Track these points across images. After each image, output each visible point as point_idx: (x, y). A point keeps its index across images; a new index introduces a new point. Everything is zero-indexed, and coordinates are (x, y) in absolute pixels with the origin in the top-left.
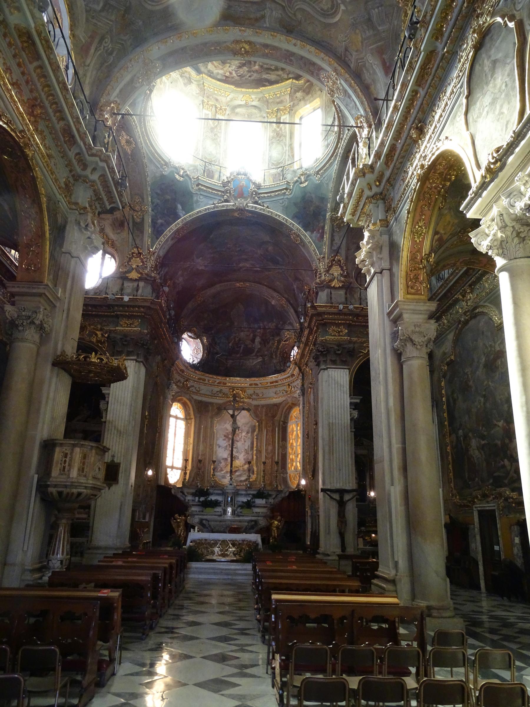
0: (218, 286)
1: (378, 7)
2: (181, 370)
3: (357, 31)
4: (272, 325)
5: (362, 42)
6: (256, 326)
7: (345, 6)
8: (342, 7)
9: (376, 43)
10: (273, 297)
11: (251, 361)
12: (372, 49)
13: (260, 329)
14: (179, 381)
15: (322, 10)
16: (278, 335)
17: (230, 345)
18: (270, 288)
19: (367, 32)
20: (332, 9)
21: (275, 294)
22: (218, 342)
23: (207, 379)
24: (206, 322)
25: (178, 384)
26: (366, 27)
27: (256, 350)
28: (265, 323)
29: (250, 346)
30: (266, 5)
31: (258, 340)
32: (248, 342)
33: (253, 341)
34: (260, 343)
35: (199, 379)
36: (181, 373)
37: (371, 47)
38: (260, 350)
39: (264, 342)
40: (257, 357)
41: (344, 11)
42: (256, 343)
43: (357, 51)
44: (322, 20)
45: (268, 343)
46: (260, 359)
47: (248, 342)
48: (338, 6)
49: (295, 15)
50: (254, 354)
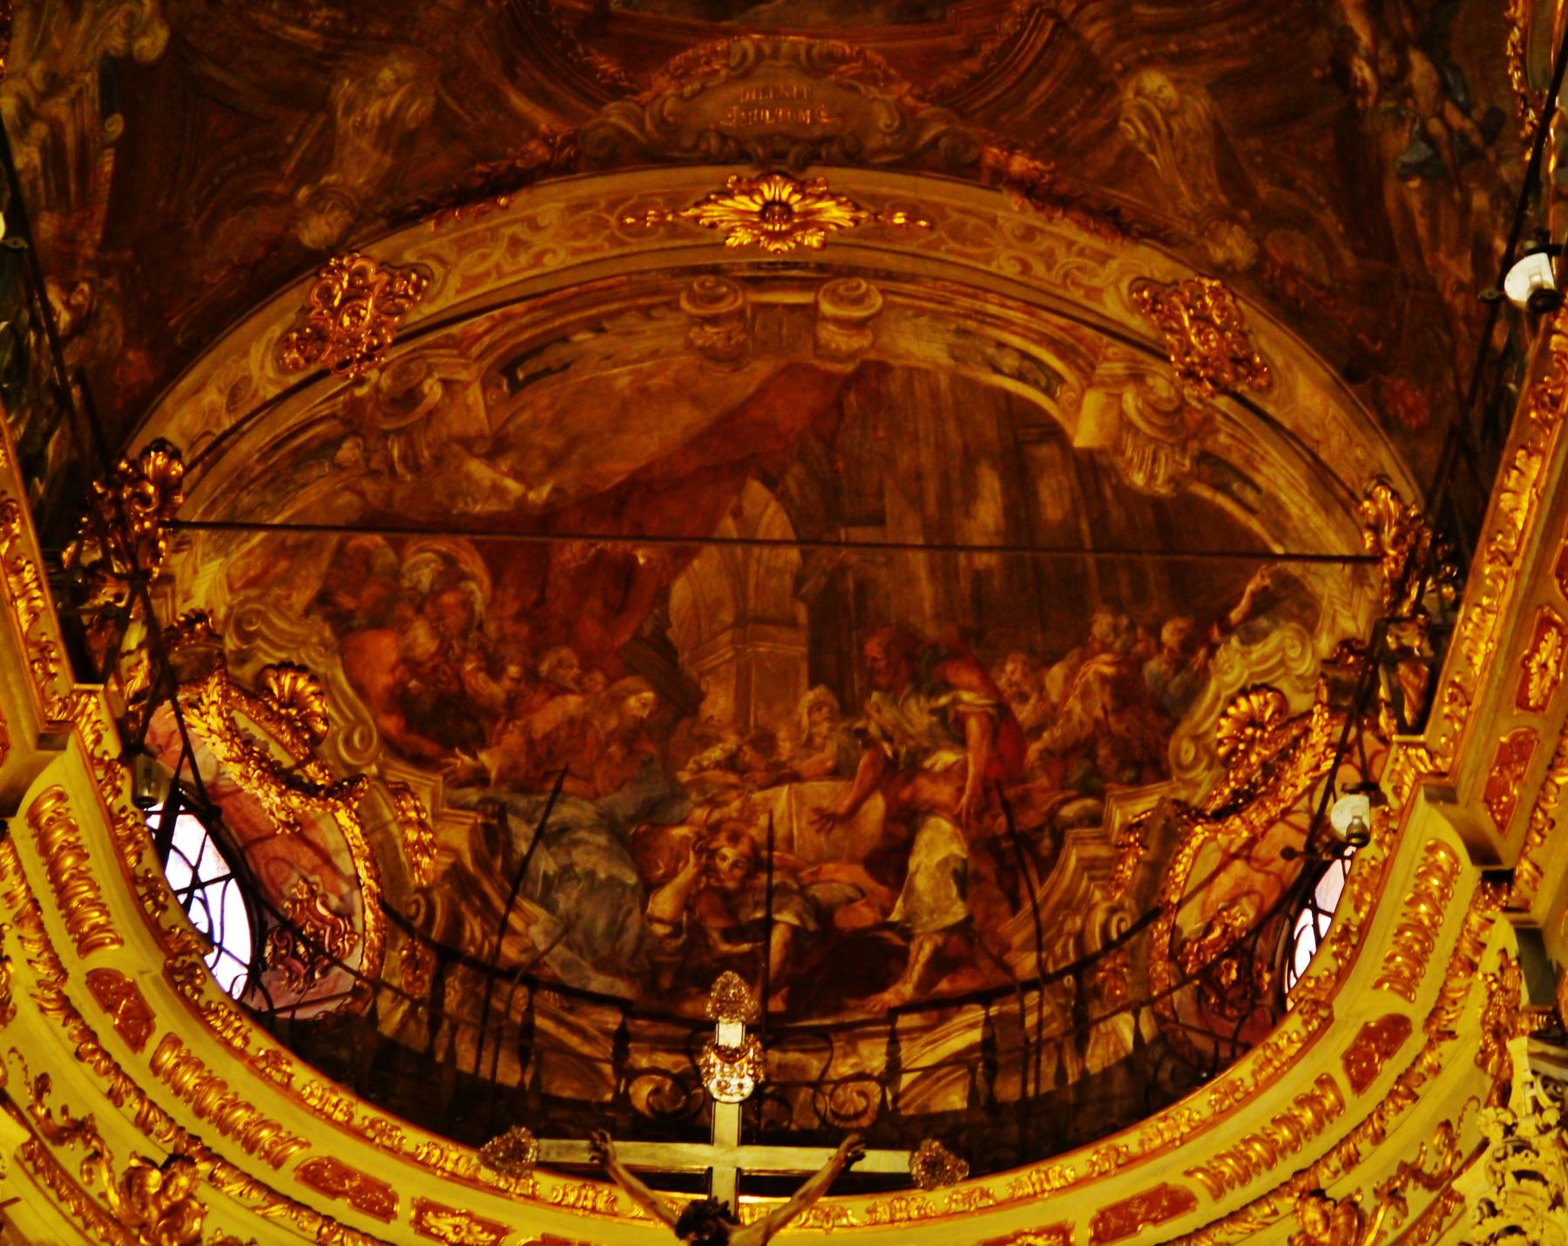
0: (549, 204)
2: (105, 985)
4: (1075, 691)
6: (919, 715)
10: (1081, 340)
11: (874, 1056)
13: (959, 740)
14: (82, 1129)
16: (1149, 765)
17: (664, 903)
21: (1114, 278)
22: (546, 864)
23: (408, 1186)
24: (422, 639)
25: (70, 1156)
27: (923, 952)
28: (1011, 671)
29: (864, 916)
31: (937, 847)
32: (841, 879)
33: (890, 860)
34: (964, 880)
35: (312, 1175)
36: (105, 1025)
38: (964, 947)
39: (1009, 857)
40: (936, 1008)
42: (921, 882)
45: (1047, 865)
46: (963, 1034)
47: (841, 879)
50: (906, 989)
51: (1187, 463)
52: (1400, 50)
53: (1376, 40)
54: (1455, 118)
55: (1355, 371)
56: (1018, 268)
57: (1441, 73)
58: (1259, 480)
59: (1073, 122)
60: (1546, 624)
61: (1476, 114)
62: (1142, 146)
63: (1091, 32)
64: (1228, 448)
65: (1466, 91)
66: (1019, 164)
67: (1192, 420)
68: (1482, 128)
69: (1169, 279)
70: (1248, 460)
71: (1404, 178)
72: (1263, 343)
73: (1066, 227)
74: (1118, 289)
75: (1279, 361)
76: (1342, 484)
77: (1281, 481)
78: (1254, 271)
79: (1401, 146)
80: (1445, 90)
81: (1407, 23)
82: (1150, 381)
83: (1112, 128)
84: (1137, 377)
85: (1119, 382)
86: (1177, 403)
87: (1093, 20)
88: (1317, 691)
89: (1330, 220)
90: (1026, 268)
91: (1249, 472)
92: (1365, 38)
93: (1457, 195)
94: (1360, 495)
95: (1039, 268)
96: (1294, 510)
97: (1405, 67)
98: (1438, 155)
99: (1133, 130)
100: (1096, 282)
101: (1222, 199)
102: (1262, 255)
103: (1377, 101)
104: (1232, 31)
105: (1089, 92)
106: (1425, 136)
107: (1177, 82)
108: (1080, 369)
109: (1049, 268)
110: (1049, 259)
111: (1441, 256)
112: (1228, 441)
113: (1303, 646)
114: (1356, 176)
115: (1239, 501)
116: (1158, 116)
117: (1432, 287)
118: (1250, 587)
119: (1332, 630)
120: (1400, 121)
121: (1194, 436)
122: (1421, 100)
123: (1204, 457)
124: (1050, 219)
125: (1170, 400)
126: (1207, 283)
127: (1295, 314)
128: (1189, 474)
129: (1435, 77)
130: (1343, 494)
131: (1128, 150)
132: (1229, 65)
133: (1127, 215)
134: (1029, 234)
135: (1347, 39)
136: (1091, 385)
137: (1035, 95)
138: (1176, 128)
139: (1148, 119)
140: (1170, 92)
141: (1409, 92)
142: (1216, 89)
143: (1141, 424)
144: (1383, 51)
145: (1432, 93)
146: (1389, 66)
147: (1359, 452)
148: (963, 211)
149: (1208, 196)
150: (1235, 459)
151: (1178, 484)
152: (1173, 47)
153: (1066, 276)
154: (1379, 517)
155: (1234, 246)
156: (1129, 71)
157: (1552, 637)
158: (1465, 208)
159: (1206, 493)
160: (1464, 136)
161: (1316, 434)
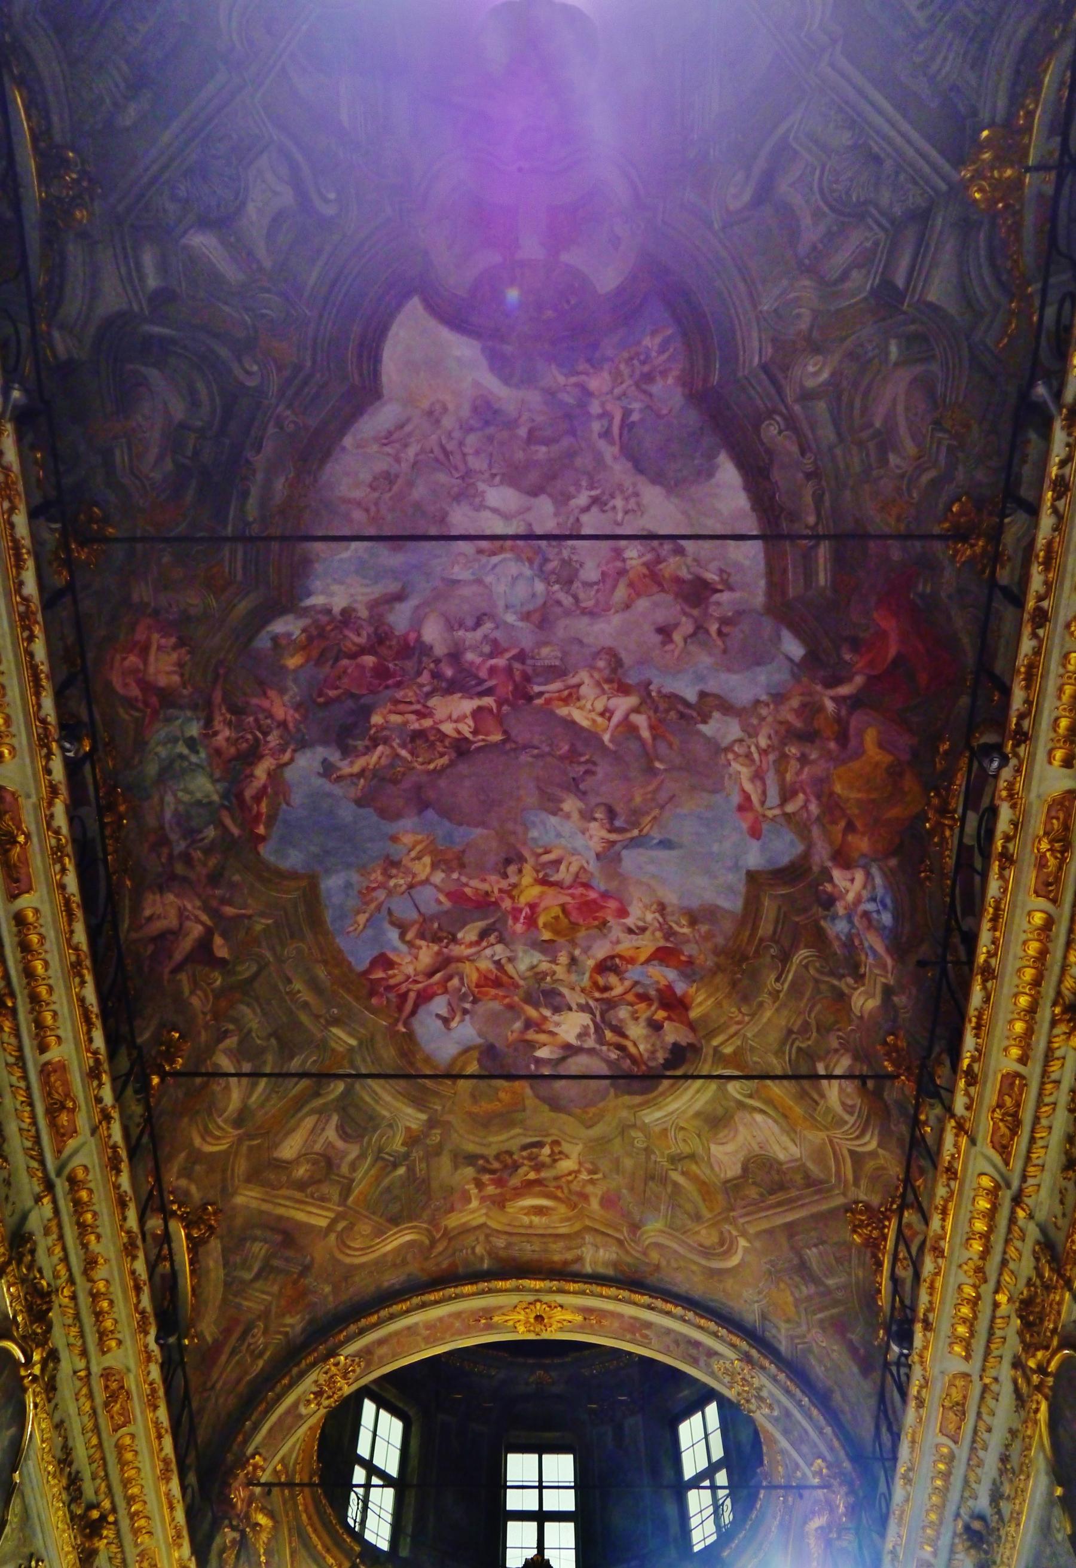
1: (816, 1246)
3: (782, 1286)
5: (796, 1307)
7: (749, 1241)
8: (743, 1242)
9: (826, 1308)
12: (821, 1321)
15: (701, 1245)
19: (804, 1288)
20: (722, 1244)
26: (797, 1279)
30: (583, 1238)
37: (820, 1316)
41: (746, 1249)
43: (788, 1321)
44: (704, 1262)
48: (733, 1242)
49: (645, 1254)
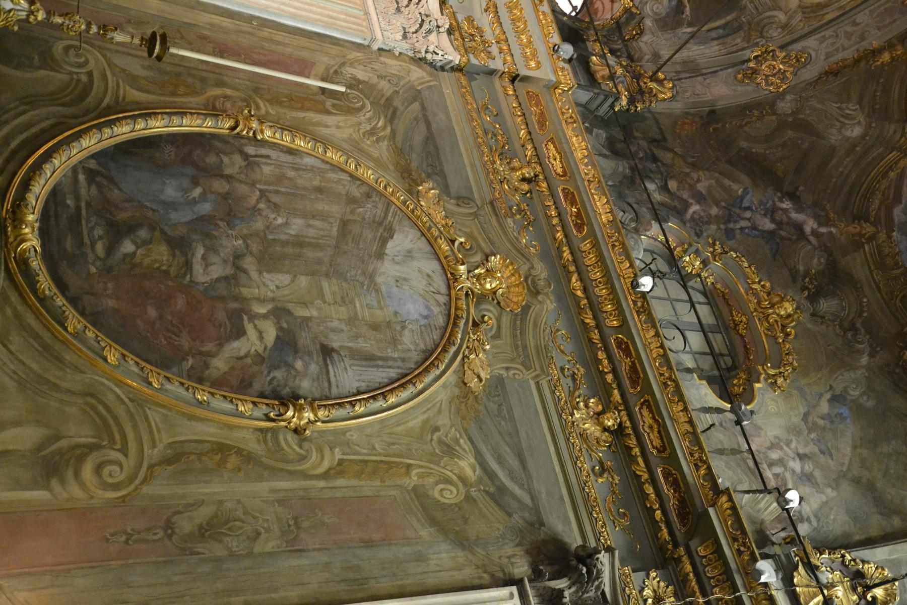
18: (857, 61)
51: (744, 19)
52: (779, 224)
53: (789, 218)
54: (744, 224)
55: (712, 117)
56: (857, 21)
57: (759, 231)
58: (716, 42)
59: (876, 91)
60: (565, 174)
61: (738, 231)
62: (844, 106)
63: (893, 127)
64: (734, 40)
65: (747, 234)
66: (886, 57)
67: (754, 34)
68: (732, 230)
69: (799, 73)
70: (724, 43)
71: (745, 189)
72: (749, 88)
73: (849, 54)
74: (814, 50)
75: (739, 88)
76: (686, 78)
77: (707, 51)
78: (772, 105)
79: (753, 198)
80: (754, 228)
81: (783, 233)
82: (779, 30)
83: (860, 102)
84: (784, 27)
85: (791, 18)
86: (764, 34)
87: (895, 132)
88: (637, 8)
89: (759, 149)
90: (855, 24)
91: (721, 41)
92: (794, 215)
93: (723, 204)
94: (676, 83)
95: (849, 29)
96: (696, 48)
97: (773, 220)
98: (740, 208)
99: (852, 108)
100: (825, 44)
101: (802, 116)
102: (774, 113)
103: (773, 201)
104: (842, 173)
105: (877, 107)
106: (749, 208)
107: (848, 138)
108: (808, 7)
109: (846, 32)
110: (848, 36)
111: (713, 181)
112: (736, 42)
113: (655, 14)
114: (760, 171)
115: (716, 28)
116: (846, 122)
117: (707, 169)
118: (688, 9)
119: (650, 29)
120: (761, 203)
121: (749, 29)
122: (759, 216)
123: (740, 28)
124: (858, 51)
125: (767, 32)
126: (785, 87)
127: (744, 110)
128: (740, 18)
129: (760, 228)
130: (683, 75)
131: (848, 101)
132: (834, 162)
133: (831, 78)
134: (862, 38)
135: (799, 210)
136: (799, 6)
137: (898, 87)
138: (837, 123)
139: (848, 117)
140: (848, 133)
141: (765, 215)
142: (833, 149)
143: (770, 13)
144: (785, 219)
145: (757, 223)
146: (779, 216)
147: (688, 94)
148: (894, 21)
149: (808, 112)
150: (729, 39)
151: (741, 9)
152: (858, 149)
153: (837, 36)
154: (663, 86)
155: (785, 106)
156: (869, 126)
157: (560, 171)
158: (717, 204)
159: (729, 18)
160: (736, 222)
161: (708, 81)
